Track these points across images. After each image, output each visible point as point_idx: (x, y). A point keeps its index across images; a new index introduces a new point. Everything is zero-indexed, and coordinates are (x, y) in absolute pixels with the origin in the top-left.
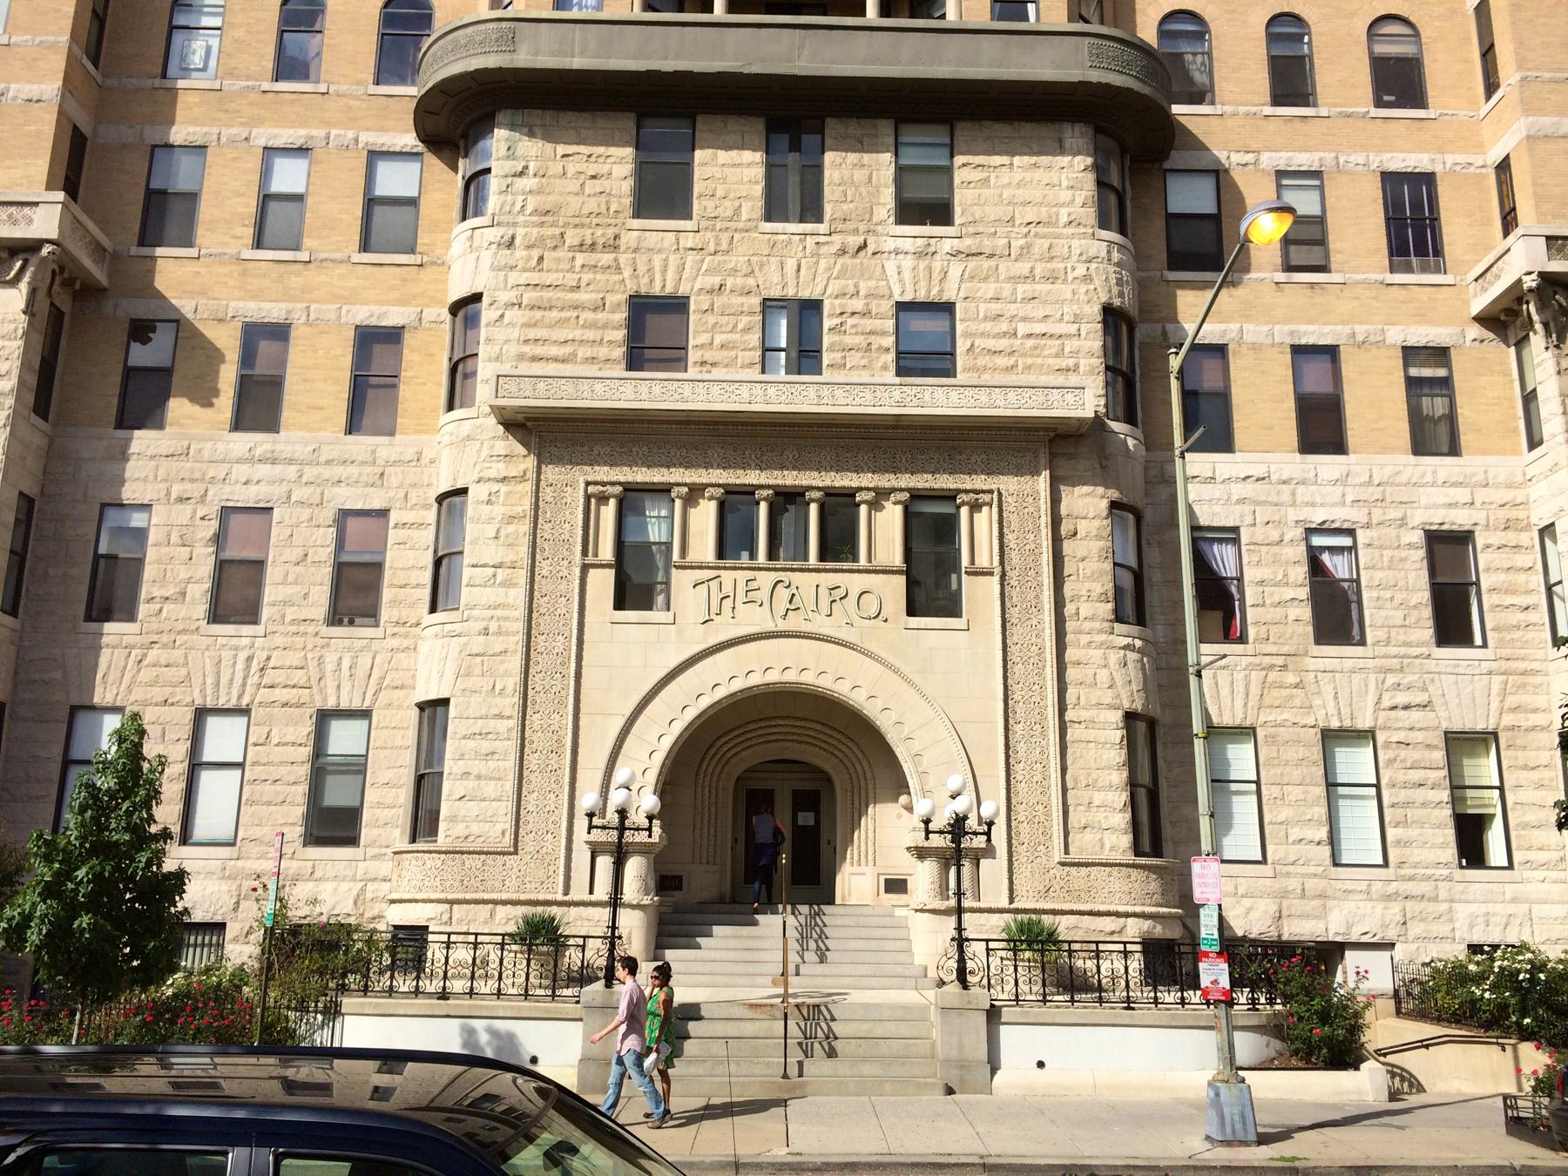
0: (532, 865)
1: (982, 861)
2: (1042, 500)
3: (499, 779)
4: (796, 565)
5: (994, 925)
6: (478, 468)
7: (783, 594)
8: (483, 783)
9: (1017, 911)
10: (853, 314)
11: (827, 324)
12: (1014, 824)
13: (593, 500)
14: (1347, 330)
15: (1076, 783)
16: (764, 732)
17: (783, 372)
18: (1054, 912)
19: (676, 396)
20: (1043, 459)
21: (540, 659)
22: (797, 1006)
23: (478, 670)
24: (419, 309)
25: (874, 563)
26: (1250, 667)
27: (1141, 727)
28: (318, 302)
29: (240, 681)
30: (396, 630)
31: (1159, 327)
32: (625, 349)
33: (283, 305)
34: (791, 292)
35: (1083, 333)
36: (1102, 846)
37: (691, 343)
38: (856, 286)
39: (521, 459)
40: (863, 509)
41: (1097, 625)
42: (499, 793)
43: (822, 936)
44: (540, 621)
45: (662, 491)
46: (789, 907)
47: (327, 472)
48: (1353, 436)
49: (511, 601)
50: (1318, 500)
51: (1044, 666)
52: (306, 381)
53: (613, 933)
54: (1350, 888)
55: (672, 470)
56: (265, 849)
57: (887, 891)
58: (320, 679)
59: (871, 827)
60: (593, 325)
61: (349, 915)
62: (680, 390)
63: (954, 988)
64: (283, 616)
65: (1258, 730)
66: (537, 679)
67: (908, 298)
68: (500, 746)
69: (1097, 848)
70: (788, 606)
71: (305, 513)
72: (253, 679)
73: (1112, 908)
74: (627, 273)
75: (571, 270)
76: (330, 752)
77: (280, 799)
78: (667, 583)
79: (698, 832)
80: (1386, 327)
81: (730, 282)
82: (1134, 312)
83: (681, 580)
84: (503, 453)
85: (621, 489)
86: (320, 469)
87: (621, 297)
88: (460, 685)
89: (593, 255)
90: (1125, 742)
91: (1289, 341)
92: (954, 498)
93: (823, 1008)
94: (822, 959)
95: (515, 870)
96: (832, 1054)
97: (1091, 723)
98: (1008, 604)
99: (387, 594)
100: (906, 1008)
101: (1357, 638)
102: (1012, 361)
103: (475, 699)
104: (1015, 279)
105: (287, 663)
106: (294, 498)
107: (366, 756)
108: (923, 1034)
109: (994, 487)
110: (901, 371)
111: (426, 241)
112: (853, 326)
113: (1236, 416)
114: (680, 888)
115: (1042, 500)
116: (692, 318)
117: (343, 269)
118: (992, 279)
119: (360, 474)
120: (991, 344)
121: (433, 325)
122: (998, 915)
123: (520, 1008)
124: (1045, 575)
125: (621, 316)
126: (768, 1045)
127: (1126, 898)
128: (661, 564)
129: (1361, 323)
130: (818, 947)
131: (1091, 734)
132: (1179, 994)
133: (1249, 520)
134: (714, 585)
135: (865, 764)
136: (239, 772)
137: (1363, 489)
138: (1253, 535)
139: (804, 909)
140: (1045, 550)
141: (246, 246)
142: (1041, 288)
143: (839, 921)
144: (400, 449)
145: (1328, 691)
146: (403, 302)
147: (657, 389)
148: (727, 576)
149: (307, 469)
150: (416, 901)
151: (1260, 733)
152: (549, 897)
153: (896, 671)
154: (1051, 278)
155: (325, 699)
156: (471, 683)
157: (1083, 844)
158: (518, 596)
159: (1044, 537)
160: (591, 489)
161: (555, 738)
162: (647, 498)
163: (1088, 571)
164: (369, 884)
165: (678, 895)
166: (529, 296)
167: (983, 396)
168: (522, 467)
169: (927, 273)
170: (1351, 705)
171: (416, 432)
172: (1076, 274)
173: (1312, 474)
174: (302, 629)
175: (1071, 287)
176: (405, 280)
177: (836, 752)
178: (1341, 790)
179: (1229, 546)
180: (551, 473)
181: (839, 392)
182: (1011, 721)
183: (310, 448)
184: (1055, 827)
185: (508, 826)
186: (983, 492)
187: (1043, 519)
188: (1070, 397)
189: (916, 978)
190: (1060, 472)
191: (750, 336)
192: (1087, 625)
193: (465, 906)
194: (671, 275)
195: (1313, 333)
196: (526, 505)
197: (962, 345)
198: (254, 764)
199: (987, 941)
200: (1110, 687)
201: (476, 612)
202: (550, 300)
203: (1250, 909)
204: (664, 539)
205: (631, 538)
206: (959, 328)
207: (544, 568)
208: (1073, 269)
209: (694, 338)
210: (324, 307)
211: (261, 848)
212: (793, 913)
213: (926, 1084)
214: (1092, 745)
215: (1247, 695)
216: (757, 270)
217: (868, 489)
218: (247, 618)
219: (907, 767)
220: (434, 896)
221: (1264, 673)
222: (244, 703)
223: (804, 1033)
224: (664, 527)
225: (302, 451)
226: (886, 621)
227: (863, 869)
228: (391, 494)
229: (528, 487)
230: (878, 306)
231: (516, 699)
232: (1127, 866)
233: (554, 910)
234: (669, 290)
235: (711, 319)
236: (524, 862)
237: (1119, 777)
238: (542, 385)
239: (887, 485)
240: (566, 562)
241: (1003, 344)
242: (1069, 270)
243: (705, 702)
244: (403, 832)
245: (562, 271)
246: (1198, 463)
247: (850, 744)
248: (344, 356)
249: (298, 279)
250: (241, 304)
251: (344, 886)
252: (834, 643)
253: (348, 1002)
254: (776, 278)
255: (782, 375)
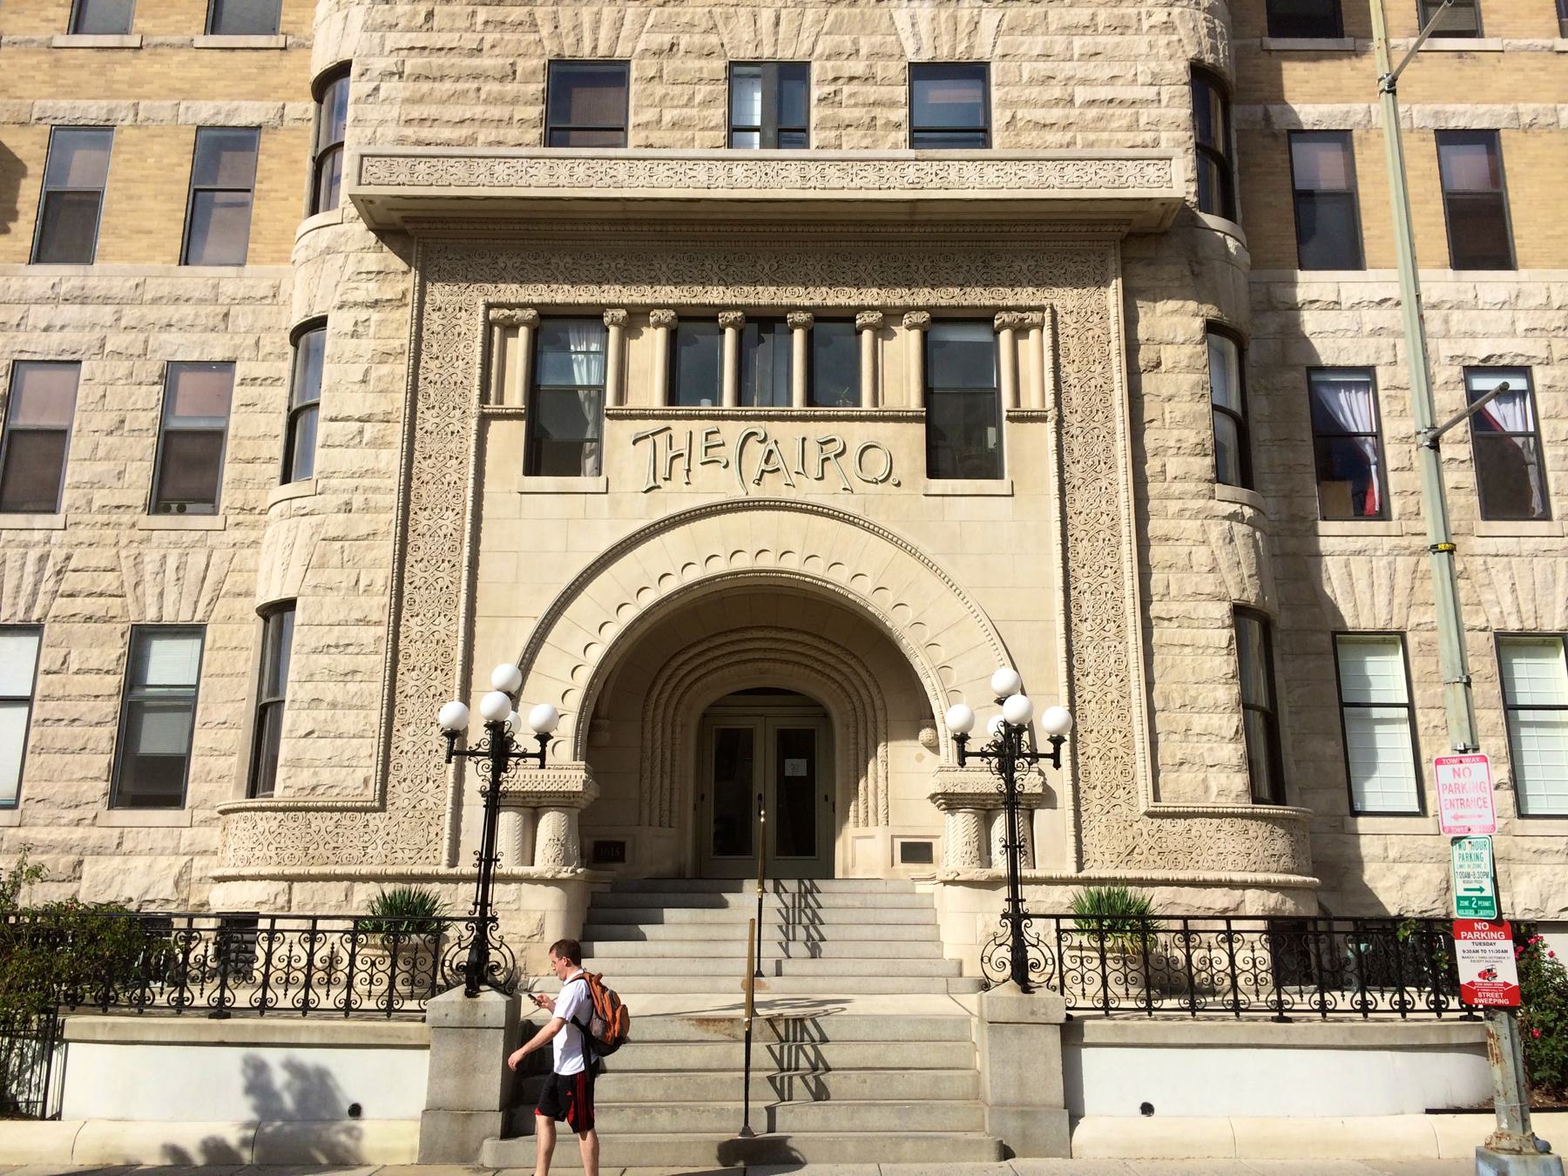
0: (405, 826)
1: (1037, 813)
2: (1113, 319)
3: (362, 707)
4: (775, 410)
5: (1061, 898)
6: (340, 289)
7: (756, 451)
8: (339, 713)
9: (1088, 882)
10: (851, 79)
11: (816, 93)
12: (1081, 760)
13: (496, 329)
14: (1509, 109)
15: (1167, 703)
16: (736, 648)
17: (757, 146)
18: (1141, 883)
19: (607, 180)
20: (1113, 265)
21: (420, 543)
22: (771, 1021)
23: (335, 560)
24: (281, 104)
25: (881, 407)
26: (1395, 552)
27: (1255, 627)
28: (149, 98)
29: (30, 588)
30: (241, 518)
31: (1259, 109)
32: (542, 130)
33: (104, 103)
34: (766, 52)
35: (1165, 98)
36: (1207, 790)
37: (632, 120)
38: (855, 42)
39: (400, 277)
40: (867, 336)
41: (1191, 487)
42: (360, 727)
43: (815, 921)
44: (423, 491)
45: (591, 317)
46: (769, 884)
47: (152, 313)
48: (1522, 246)
49: (382, 465)
50: (1480, 328)
51: (1119, 543)
52: (130, 198)
53: (483, 912)
54: (1543, 847)
55: (605, 287)
56: (56, 812)
57: (905, 859)
58: (137, 585)
59: (881, 773)
60: (499, 100)
61: (168, 901)
62: (612, 172)
63: (1010, 990)
64: (90, 502)
65: (1409, 636)
66: (416, 570)
67: (925, 57)
68: (363, 662)
69: (1200, 792)
70: (764, 467)
71: (123, 367)
72: (47, 586)
73: (1224, 876)
74: (545, 31)
75: (471, 28)
76: (150, 681)
77: (79, 745)
78: (598, 440)
79: (646, 783)
80: (1560, 106)
81: (684, 41)
82: (1231, 75)
83: (616, 434)
84: (375, 268)
85: (534, 312)
86: (145, 309)
87: (537, 63)
88: (311, 579)
89: (500, 9)
90: (1234, 646)
91: (1432, 124)
92: (991, 320)
93: (809, 1024)
94: (815, 952)
95: (382, 833)
96: (821, 1094)
97: (1186, 620)
98: (1067, 460)
99: (229, 472)
100: (934, 1021)
101: (1538, 510)
102: (1068, 136)
103: (331, 599)
104: (1070, 30)
105: (93, 564)
106: (108, 348)
107: (197, 686)
108: (962, 1063)
109: (1044, 302)
110: (913, 143)
111: (291, 17)
112: (852, 95)
113: (1365, 223)
114: (621, 859)
115: (1113, 319)
116: (634, 88)
117: (183, 55)
118: (1039, 30)
119: (197, 315)
120: (1039, 114)
121: (299, 124)
122: (1061, 888)
123: (334, 1029)
124: (1118, 419)
125: (537, 87)
126: (722, 1082)
127: (1242, 862)
128: (590, 417)
129: (1525, 101)
130: (809, 936)
131: (1187, 635)
132: (1317, 997)
133: (1387, 357)
134: (661, 440)
135: (874, 690)
136: (25, 710)
137: (1538, 312)
138: (1394, 376)
139: (791, 885)
140: (1116, 385)
141: (60, 30)
142: (1107, 41)
143: (840, 901)
144: (250, 282)
145: (1502, 581)
146: (260, 96)
147: (581, 170)
148: (680, 428)
149: (127, 310)
150: (243, 878)
151: (1412, 639)
152: (428, 870)
153: (913, 552)
154: (1120, 28)
155: (143, 612)
156: (324, 577)
157: (1180, 788)
158: (391, 459)
159: (1115, 369)
160: (493, 314)
161: (441, 650)
162: (571, 324)
163: (1178, 415)
164: (197, 859)
165: (619, 867)
166: (413, 63)
167: (1030, 173)
168: (400, 287)
169: (951, 23)
170: (1534, 600)
171: (273, 261)
172: (1155, 20)
173: (1471, 296)
174: (114, 518)
175: (1147, 38)
176: (264, 68)
177: (834, 674)
178: (1524, 715)
179: (1361, 394)
180: (439, 293)
181: (831, 171)
182: (1075, 619)
183: (133, 282)
184: (1140, 764)
185: (372, 772)
186: (1031, 309)
187: (1114, 346)
188: (1151, 171)
189: (946, 977)
190: (1137, 283)
191: (712, 111)
192: (1177, 487)
193: (310, 884)
194: (605, 33)
195: (1464, 113)
196: (404, 338)
197: (999, 118)
198: (46, 698)
199: (1058, 917)
200: (1212, 570)
201: (334, 482)
202: (441, 67)
203: (1407, 878)
204: (594, 382)
205: (549, 380)
206: (996, 95)
207: (427, 419)
208: (1150, 15)
209: (636, 114)
210: (157, 103)
211: (50, 812)
212: (776, 891)
213: (969, 1143)
214: (1187, 650)
215: (1392, 588)
216: (720, 25)
217: (872, 308)
218: (45, 506)
219: (930, 684)
220: (265, 871)
221: (1414, 559)
222: (35, 615)
223: (779, 1062)
224: (595, 367)
225: (121, 286)
226: (898, 485)
227: (871, 830)
228: (238, 340)
229: (406, 314)
230: (885, 68)
231: (386, 599)
232: (1243, 816)
233: (432, 889)
234: (602, 51)
235: (659, 90)
236: (393, 822)
237: (1228, 694)
238: (422, 168)
239: (898, 302)
240: (458, 413)
241: (1055, 114)
242: (1144, 16)
243: (649, 599)
244: (237, 787)
245: (458, 30)
246: (1311, 284)
247: (852, 662)
248: (181, 165)
249: (124, 70)
250: (50, 103)
251: (163, 862)
252: (827, 515)
253: (74, 1023)
254: (747, 34)
255: (756, 150)
